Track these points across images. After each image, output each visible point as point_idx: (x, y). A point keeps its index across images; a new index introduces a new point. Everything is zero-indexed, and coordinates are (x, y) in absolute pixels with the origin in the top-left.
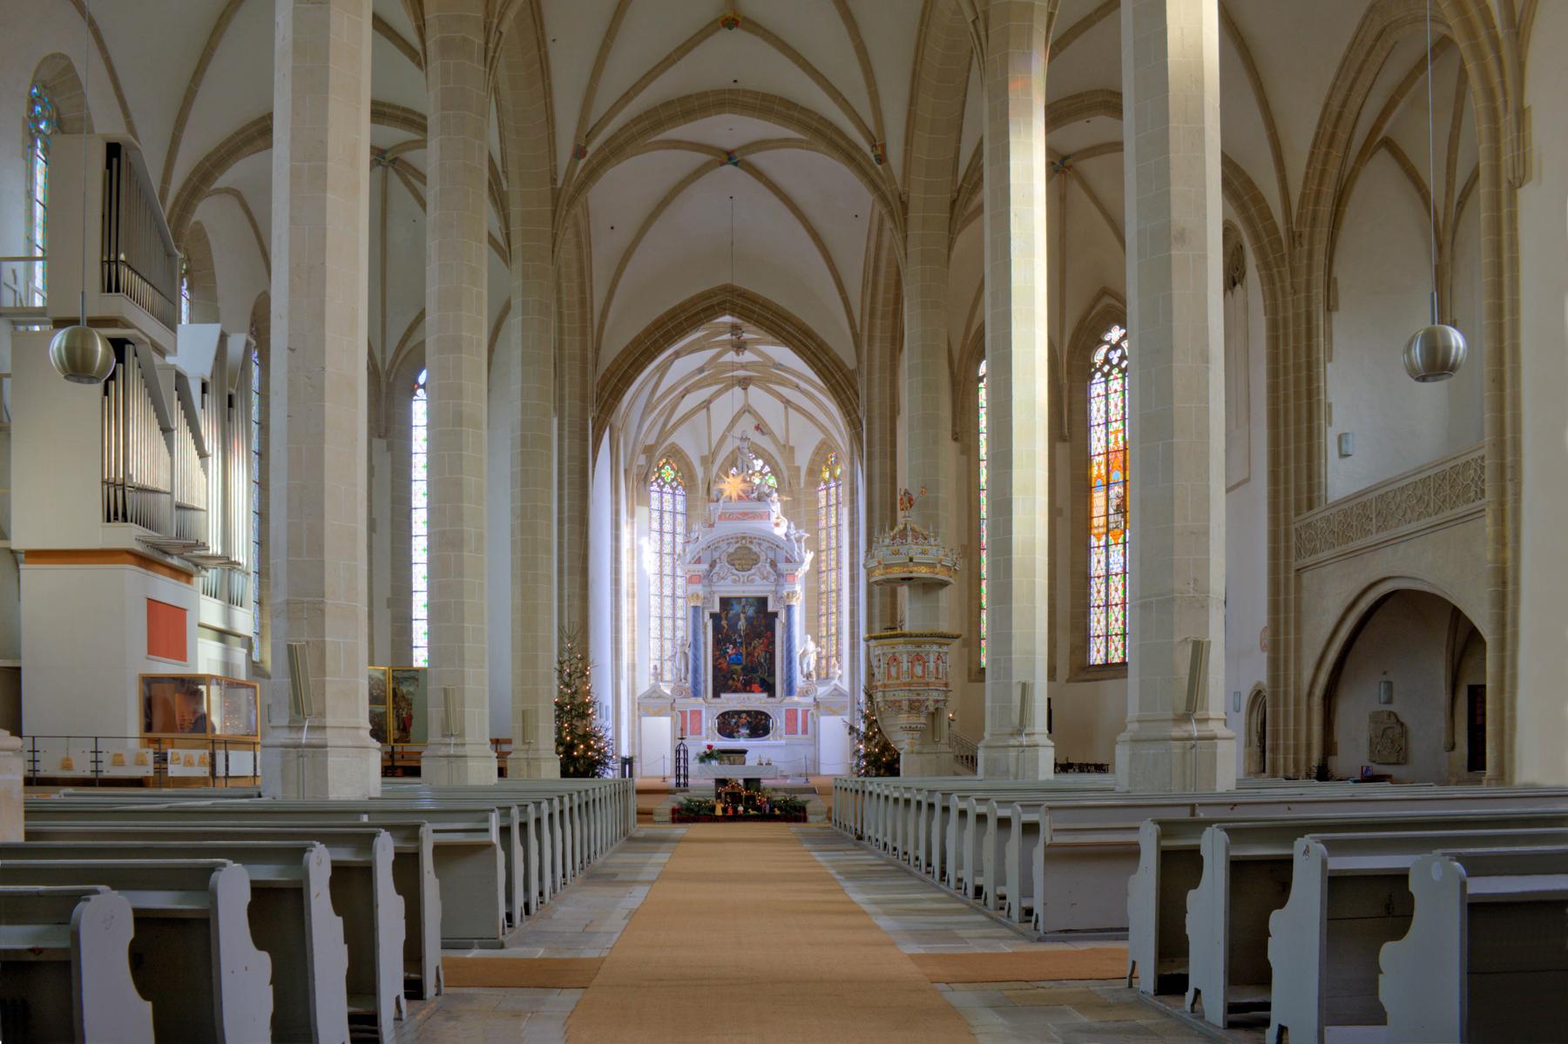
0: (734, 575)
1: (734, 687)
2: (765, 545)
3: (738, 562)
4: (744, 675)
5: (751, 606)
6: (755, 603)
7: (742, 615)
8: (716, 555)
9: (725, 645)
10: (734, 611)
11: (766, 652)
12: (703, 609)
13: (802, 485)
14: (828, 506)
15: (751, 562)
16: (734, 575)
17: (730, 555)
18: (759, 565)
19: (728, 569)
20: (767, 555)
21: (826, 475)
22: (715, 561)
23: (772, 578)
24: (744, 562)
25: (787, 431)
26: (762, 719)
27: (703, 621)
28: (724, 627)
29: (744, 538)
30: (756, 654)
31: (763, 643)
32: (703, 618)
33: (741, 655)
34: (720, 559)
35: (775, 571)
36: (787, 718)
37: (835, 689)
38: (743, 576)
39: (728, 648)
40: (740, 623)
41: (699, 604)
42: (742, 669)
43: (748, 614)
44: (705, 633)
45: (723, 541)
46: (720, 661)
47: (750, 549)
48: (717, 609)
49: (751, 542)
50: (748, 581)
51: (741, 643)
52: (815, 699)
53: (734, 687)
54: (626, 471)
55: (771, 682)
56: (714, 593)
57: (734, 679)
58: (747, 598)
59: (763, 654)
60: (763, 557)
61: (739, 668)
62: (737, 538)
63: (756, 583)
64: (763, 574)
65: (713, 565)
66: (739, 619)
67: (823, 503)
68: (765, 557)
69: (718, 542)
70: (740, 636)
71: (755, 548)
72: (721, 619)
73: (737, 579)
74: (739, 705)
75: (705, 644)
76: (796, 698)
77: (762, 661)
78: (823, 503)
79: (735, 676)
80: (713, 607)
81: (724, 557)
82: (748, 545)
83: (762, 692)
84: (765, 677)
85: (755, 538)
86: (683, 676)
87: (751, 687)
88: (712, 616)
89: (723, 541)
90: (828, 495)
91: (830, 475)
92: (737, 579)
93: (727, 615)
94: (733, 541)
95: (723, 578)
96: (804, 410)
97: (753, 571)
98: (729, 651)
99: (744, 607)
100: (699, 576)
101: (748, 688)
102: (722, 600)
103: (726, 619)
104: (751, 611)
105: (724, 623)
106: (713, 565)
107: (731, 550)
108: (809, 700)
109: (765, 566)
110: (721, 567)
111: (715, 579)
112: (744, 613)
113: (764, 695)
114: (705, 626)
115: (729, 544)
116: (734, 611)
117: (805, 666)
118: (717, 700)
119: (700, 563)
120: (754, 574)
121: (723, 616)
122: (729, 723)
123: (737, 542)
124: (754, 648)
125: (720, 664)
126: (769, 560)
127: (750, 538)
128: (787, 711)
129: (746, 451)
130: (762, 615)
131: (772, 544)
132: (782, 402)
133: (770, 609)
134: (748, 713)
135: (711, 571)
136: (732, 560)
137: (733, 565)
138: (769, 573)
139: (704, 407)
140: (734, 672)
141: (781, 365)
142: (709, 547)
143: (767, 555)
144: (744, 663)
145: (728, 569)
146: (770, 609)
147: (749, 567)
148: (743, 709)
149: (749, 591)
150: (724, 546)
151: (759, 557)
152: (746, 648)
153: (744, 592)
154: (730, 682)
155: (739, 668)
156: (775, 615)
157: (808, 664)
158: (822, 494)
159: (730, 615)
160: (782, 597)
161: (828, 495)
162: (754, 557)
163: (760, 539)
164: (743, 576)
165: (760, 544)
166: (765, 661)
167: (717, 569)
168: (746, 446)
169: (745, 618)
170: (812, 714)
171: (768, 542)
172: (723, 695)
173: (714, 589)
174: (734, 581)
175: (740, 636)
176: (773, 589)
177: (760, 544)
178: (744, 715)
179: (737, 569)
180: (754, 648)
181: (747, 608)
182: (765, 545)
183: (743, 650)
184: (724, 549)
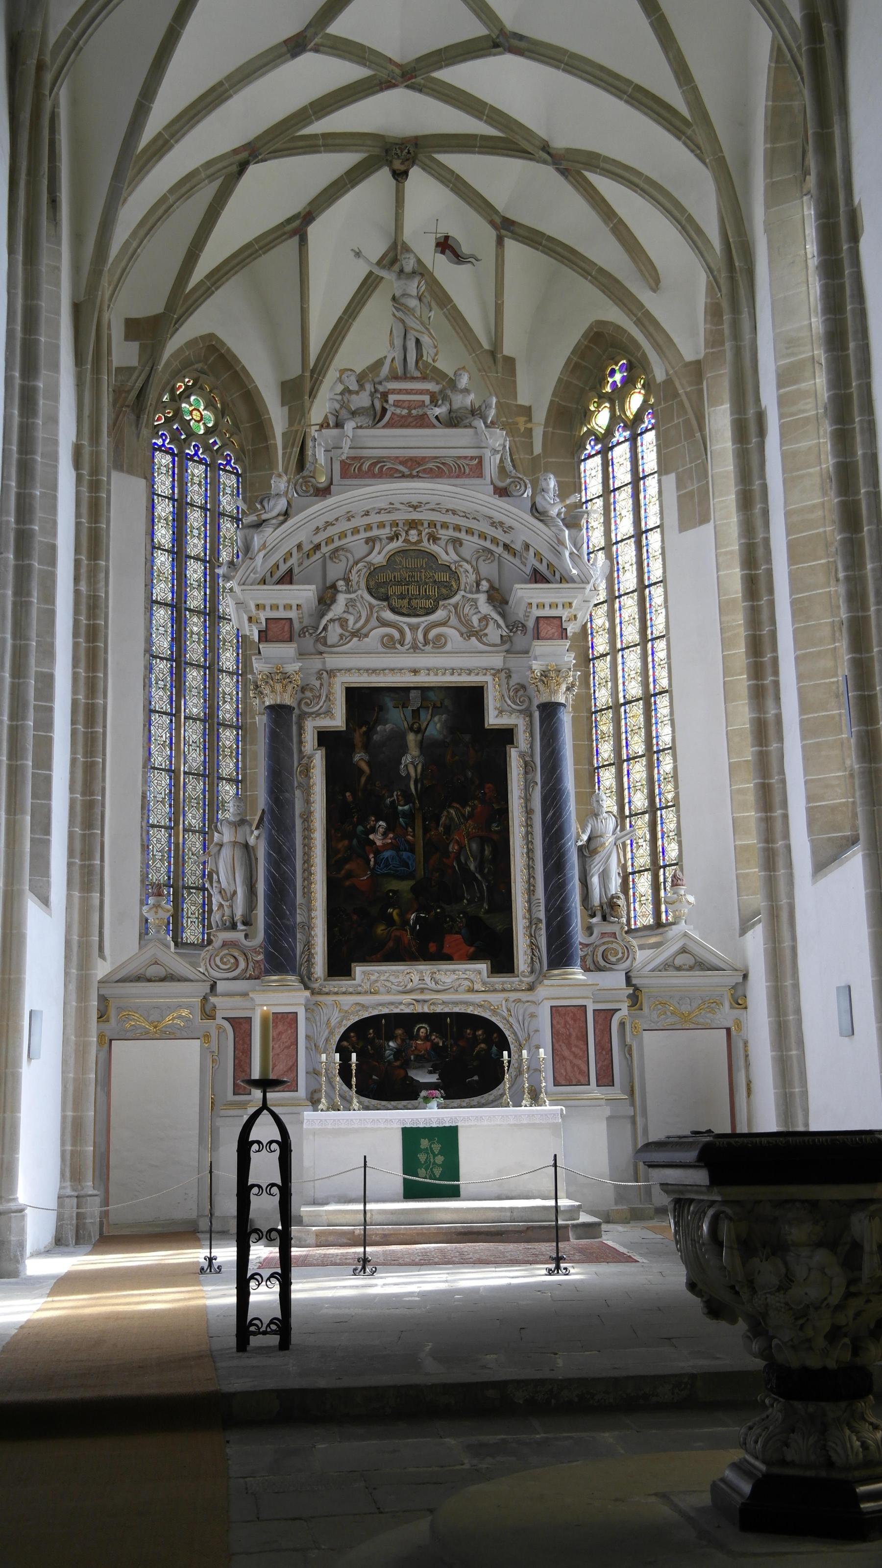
0: (385, 624)
1: (391, 944)
2: (471, 543)
3: (398, 590)
4: (418, 911)
5: (436, 709)
6: (447, 702)
7: (411, 738)
8: (335, 571)
9: (363, 820)
10: (388, 727)
11: (483, 841)
12: (302, 716)
13: (538, 449)
14: (608, 491)
15: (432, 591)
16: (385, 624)
17: (374, 572)
18: (453, 601)
19: (372, 607)
20: (478, 573)
21: (601, 419)
22: (334, 586)
23: (494, 634)
24: (413, 590)
25: (499, 309)
26: (475, 1041)
27: (300, 751)
28: (361, 772)
29: (413, 524)
30: (453, 848)
31: (471, 816)
32: (300, 742)
33: (412, 849)
34: (347, 580)
35: (503, 615)
36: (555, 1034)
37: (684, 950)
38: (414, 628)
39: (373, 830)
40: (407, 759)
41: (288, 700)
42: (413, 889)
43: (427, 733)
44: (307, 790)
45: (355, 531)
46: (347, 867)
47: (433, 557)
48: (337, 721)
49: (433, 538)
50: (426, 642)
51: (410, 816)
52: (628, 979)
53: (391, 944)
54: (77, 309)
55: (499, 927)
56: (331, 673)
57: (390, 922)
58: (424, 690)
59: (474, 846)
60: (468, 578)
61: (404, 886)
62: (395, 524)
63: (448, 648)
64: (467, 623)
65: (327, 598)
66: (404, 749)
67: (594, 486)
68: (473, 577)
69: (343, 535)
70: (407, 798)
71: (446, 555)
72: (351, 748)
73: (397, 635)
74: (407, 998)
75: (307, 817)
76: (577, 974)
77: (472, 867)
78: (594, 486)
79: (395, 913)
80: (329, 713)
81: (358, 577)
82: (428, 546)
83: (474, 957)
84: (481, 914)
85: (445, 526)
86: (239, 912)
87: (441, 947)
88: (325, 738)
89: (355, 531)
90: (606, 465)
91: (613, 417)
92: (397, 635)
93: (368, 735)
94: (386, 531)
95: (356, 634)
96: (550, 239)
97: (440, 615)
98: (377, 838)
99: (416, 713)
100: (291, 619)
101: (432, 947)
102: (354, 695)
103: (366, 747)
104: (435, 727)
105: (359, 757)
106: (327, 598)
107: (378, 558)
108: (615, 980)
109: (475, 601)
110: (350, 604)
111: (334, 633)
112: (418, 731)
113: (483, 967)
114: (307, 771)
115: (371, 541)
116: (388, 727)
117: (595, 880)
118: (343, 984)
119: (291, 583)
120: (444, 624)
121: (358, 738)
122: (380, 1051)
123: (397, 536)
124: (448, 829)
125: (350, 875)
126: (485, 585)
127: (432, 524)
128: (555, 1011)
129: (413, 303)
130: (467, 738)
131: (495, 541)
132: (492, 223)
133: (493, 719)
134: (435, 1020)
135: (322, 615)
136: (379, 585)
137: (386, 598)
138: (485, 619)
139: (294, 233)
140: (393, 899)
141: (521, 37)
142: (318, 547)
143: (478, 573)
144: (420, 873)
145: (372, 607)
146: (493, 719)
147: (428, 604)
148: (420, 1009)
149: (435, 670)
150: (357, 544)
151: (455, 575)
152: (426, 830)
153: (415, 672)
154: (380, 929)
155: (404, 886)
156: (506, 736)
157: (604, 876)
158: (592, 468)
159: (376, 737)
160: (523, 687)
161: (606, 465)
162: (444, 577)
163: (458, 528)
164: (414, 628)
165: (457, 543)
166: (480, 868)
167: (338, 609)
168: (414, 292)
169: (421, 745)
170: (622, 1024)
171: (483, 536)
172: (359, 970)
173: (332, 662)
174: (389, 644)
175: (407, 798)
176: (497, 661)
177: (457, 543)
178: (423, 1029)
179: (394, 610)
180: (448, 829)
181: (424, 716)
182: (471, 543)
183: (416, 836)
184: (358, 555)
